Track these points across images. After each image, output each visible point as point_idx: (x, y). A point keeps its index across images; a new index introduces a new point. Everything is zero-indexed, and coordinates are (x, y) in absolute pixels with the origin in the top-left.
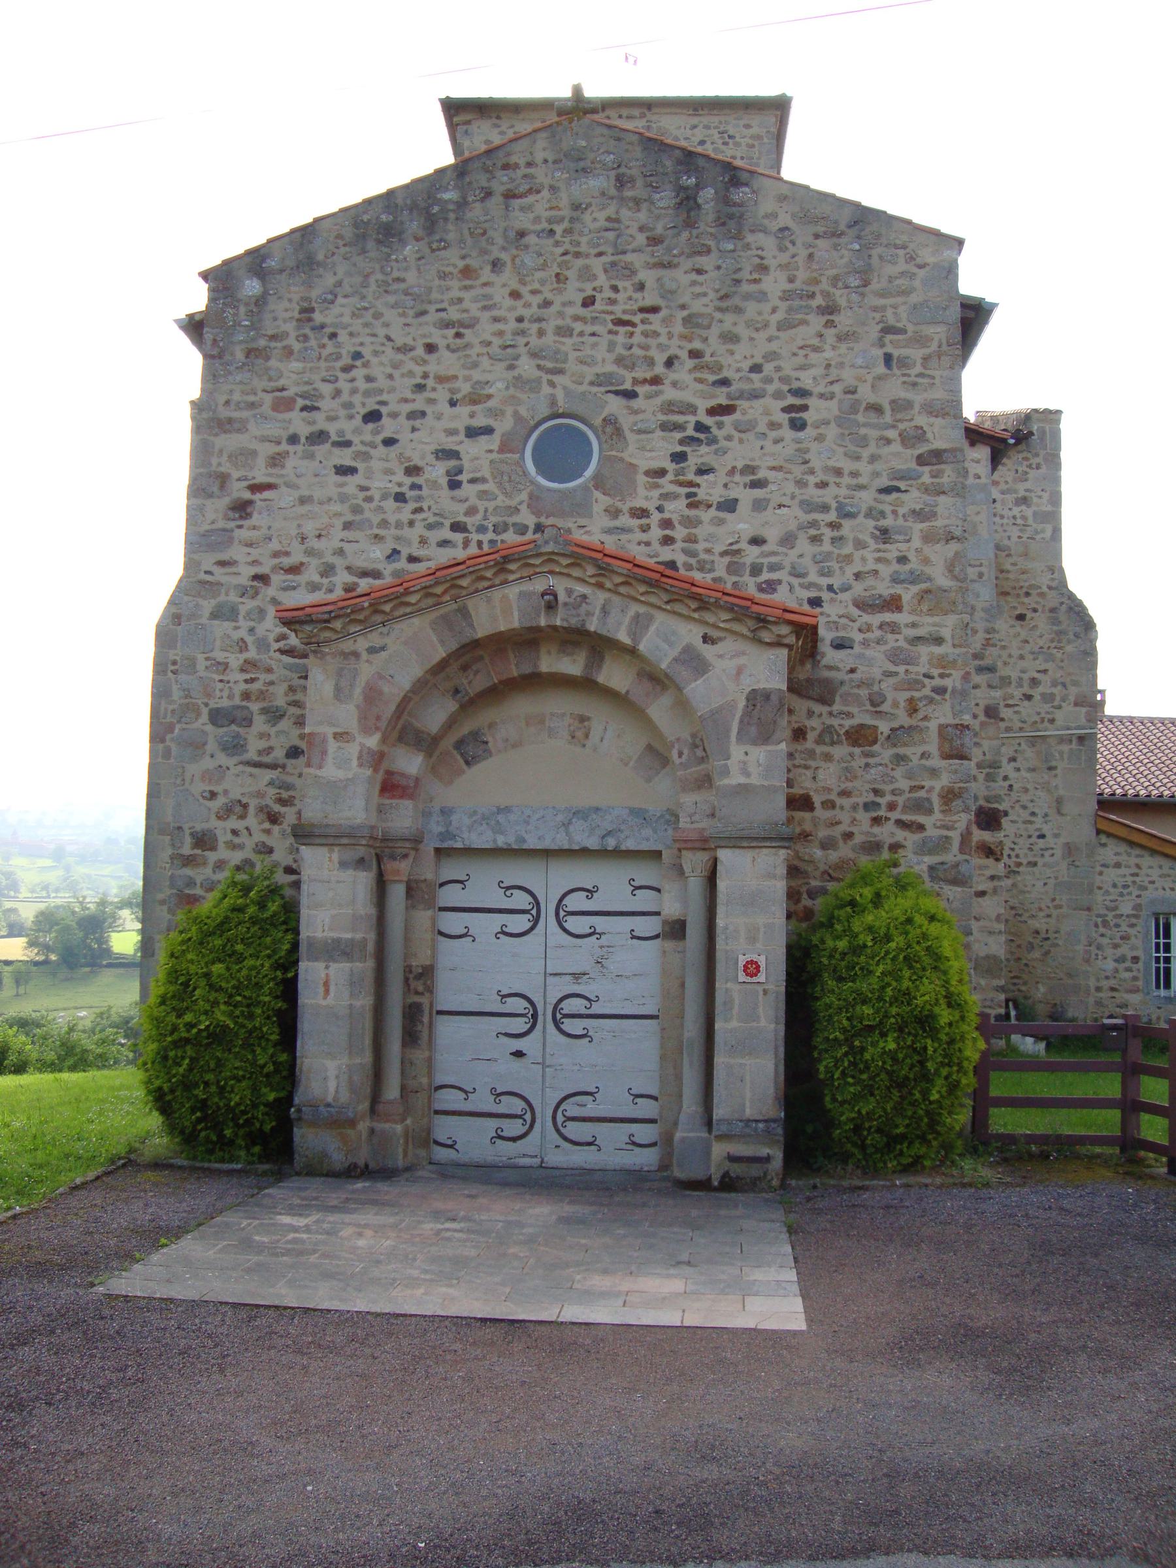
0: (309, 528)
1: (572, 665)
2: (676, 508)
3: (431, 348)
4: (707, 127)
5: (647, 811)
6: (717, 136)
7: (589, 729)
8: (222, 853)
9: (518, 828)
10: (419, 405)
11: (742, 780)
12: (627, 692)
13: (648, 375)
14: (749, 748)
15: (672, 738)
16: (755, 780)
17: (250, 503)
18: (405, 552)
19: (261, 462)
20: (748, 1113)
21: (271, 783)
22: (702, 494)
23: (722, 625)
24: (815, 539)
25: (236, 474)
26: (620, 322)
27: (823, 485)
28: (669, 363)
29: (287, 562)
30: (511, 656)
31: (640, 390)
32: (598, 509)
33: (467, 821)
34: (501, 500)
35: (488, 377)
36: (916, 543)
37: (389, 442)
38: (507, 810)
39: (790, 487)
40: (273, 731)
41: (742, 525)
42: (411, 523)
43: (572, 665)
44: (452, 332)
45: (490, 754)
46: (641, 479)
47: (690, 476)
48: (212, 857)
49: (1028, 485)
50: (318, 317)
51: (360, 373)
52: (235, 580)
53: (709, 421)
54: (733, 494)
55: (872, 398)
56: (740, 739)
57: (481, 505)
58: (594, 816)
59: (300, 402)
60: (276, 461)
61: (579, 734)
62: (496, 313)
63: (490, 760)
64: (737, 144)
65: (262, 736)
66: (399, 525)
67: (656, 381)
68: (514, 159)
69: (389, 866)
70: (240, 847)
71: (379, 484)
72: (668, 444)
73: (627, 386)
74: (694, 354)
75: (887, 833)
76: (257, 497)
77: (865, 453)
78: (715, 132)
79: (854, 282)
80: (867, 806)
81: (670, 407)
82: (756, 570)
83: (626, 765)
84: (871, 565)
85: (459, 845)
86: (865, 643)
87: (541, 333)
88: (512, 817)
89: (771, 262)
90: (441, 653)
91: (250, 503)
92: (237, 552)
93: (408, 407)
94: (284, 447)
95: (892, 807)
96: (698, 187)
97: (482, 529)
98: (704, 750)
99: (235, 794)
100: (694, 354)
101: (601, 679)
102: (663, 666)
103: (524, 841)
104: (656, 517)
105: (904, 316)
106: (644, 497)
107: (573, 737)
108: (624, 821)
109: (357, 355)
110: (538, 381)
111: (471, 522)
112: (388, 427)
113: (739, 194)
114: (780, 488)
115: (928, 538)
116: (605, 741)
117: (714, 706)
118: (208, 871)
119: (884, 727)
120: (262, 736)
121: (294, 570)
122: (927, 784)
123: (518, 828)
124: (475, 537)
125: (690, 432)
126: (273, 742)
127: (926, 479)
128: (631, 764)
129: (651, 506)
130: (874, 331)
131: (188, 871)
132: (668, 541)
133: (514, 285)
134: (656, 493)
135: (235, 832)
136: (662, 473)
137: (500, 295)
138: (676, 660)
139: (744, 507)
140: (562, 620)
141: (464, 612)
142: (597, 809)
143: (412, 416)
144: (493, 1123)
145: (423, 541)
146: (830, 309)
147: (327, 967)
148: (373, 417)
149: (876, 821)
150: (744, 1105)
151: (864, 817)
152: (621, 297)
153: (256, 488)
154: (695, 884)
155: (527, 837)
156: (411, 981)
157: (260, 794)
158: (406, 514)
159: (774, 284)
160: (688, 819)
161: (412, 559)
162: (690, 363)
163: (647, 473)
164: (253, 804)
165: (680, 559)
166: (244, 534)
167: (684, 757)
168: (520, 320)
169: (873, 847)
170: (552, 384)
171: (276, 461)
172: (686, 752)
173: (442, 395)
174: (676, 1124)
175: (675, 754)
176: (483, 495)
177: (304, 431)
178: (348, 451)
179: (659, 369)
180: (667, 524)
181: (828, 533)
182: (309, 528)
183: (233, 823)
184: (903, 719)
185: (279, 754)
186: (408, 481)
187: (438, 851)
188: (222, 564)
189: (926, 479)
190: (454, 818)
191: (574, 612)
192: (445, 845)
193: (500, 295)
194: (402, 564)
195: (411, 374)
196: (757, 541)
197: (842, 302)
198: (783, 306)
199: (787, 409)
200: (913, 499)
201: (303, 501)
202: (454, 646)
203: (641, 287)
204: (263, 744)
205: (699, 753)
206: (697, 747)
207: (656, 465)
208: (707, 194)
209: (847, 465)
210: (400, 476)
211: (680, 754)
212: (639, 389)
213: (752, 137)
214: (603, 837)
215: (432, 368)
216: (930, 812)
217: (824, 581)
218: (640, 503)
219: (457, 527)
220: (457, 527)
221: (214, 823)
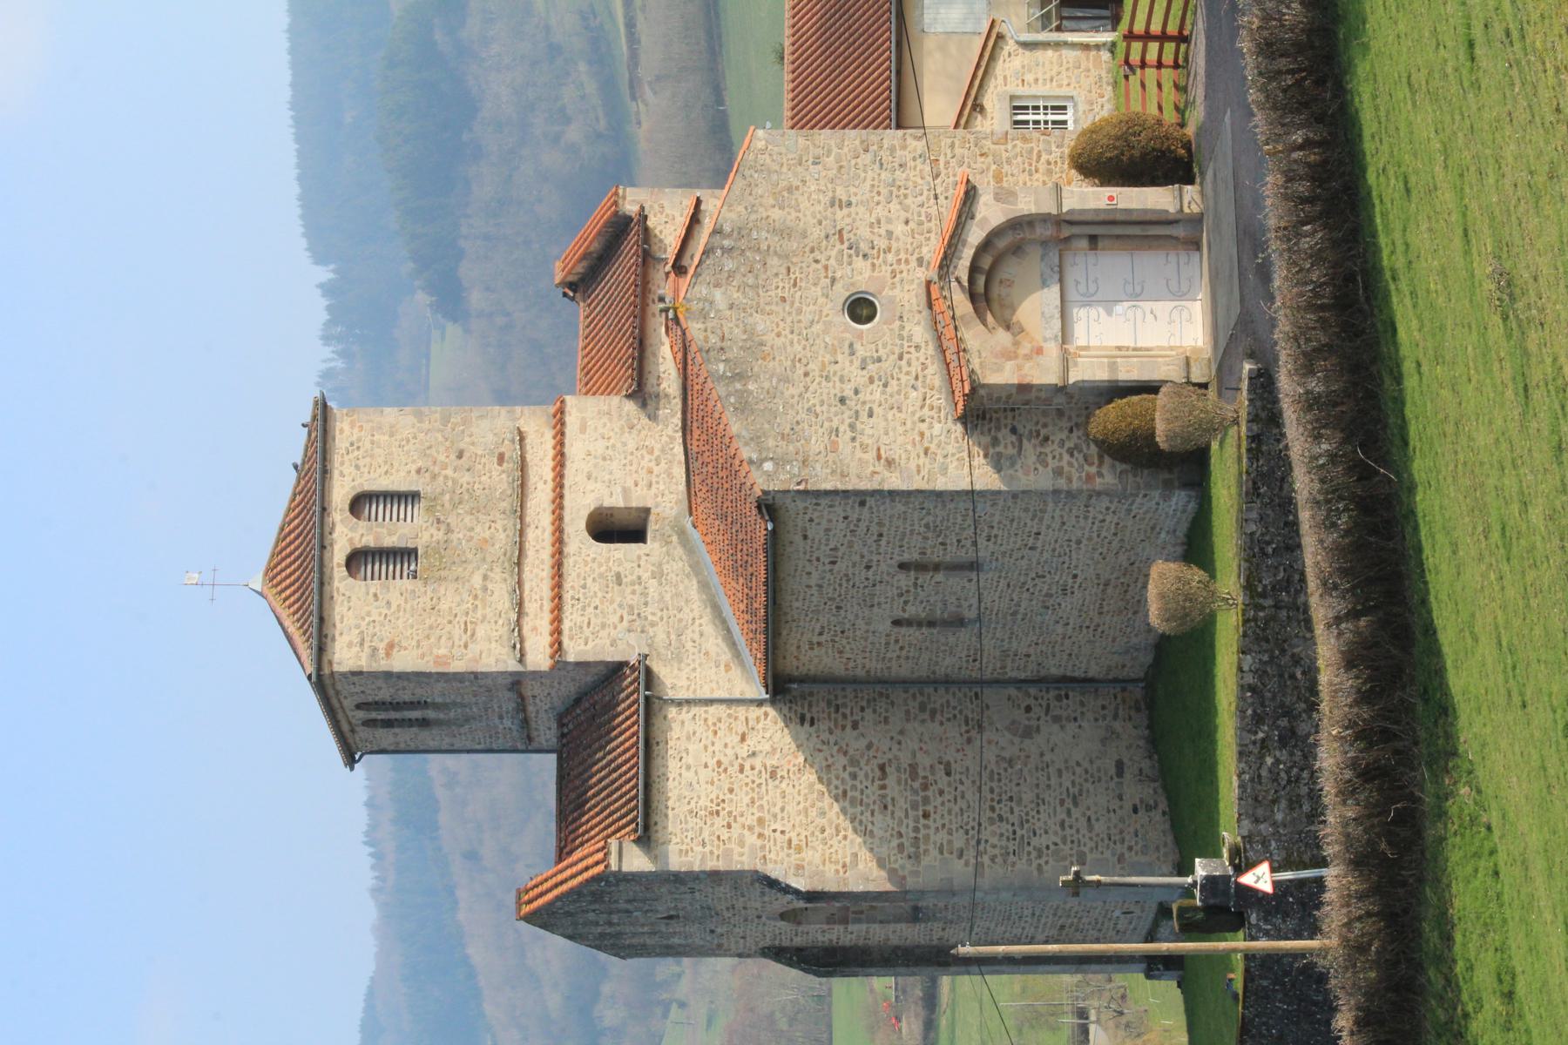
0: (901, 429)
1: (981, 280)
2: (890, 257)
3: (806, 374)
4: (342, 464)
6: (351, 456)
8: (1064, 463)
10: (837, 379)
13: (823, 271)
16: (1032, 199)
17: (887, 460)
18: (913, 382)
19: (865, 456)
20: (1171, 199)
21: (1029, 440)
22: (883, 247)
24: (906, 196)
25: (871, 468)
26: (795, 285)
27: (879, 193)
28: (817, 261)
29: (918, 438)
31: (830, 275)
32: (890, 293)
34: (887, 338)
35: (823, 345)
36: (906, 153)
37: (856, 392)
39: (880, 207)
40: (1003, 442)
41: (899, 229)
42: (898, 379)
43: (981, 280)
44: (798, 365)
46: (876, 274)
47: (875, 251)
48: (1066, 469)
49: (677, 214)
50: (787, 431)
51: (818, 409)
52: (928, 466)
53: (846, 244)
54: (883, 233)
55: (834, 172)
57: (889, 347)
59: (833, 437)
60: (864, 448)
62: (788, 343)
64: (359, 440)
65: (1006, 447)
66: (899, 385)
67: (826, 268)
68: (701, 337)
70: (1061, 454)
71: (877, 396)
72: (859, 263)
73: (828, 281)
74: (812, 251)
75: (1042, 167)
76: (884, 456)
77: (863, 175)
78: (346, 458)
79: (775, 177)
80: (1031, 175)
81: (840, 263)
82: (920, 224)
84: (918, 172)
86: (954, 175)
87: (799, 321)
89: (764, 215)
91: (887, 460)
92: (913, 466)
93: (838, 384)
94: (857, 444)
95: (1031, 165)
96: (722, 248)
97: (902, 345)
99: (1034, 458)
100: (812, 251)
101: (986, 267)
104: (895, 266)
105: (790, 156)
106: (886, 271)
109: (809, 410)
110: (824, 322)
111: (897, 351)
112: (848, 393)
113: (727, 229)
114: (880, 211)
115: (904, 147)
118: (1073, 470)
119: (994, 167)
120: (1006, 447)
121: (922, 434)
122: (1018, 150)
124: (906, 349)
125: (852, 252)
126: (1008, 441)
127: (875, 147)
129: (890, 269)
130: (799, 169)
131: (1075, 479)
132: (907, 261)
133: (773, 335)
134: (884, 268)
135: (1054, 457)
136: (873, 265)
137: (779, 342)
139: (890, 227)
141: (962, 317)
143: (842, 380)
145: (908, 373)
146: (790, 189)
148: (842, 400)
149: (1037, 171)
151: (1036, 176)
152: (781, 285)
153: (879, 457)
154: (1076, 230)
157: (1035, 446)
158: (894, 382)
159: (776, 214)
161: (917, 378)
162: (817, 252)
163: (873, 270)
164: (1039, 449)
165: (916, 256)
166: (903, 462)
168: (792, 332)
169: (1049, 172)
170: (827, 315)
171: (864, 448)
173: (833, 368)
174: (1177, 238)
176: (885, 346)
177: (849, 434)
178: (861, 413)
179: (819, 266)
180: (899, 261)
181: (902, 191)
182: (901, 429)
183: (1049, 459)
184: (991, 158)
185: (1014, 438)
186: (877, 382)
188: (919, 472)
189: (875, 147)
193: (779, 342)
194: (919, 383)
195: (819, 384)
196: (907, 222)
197: (785, 183)
198: (787, 210)
199: (841, 207)
200: (885, 154)
201: (887, 433)
203: (777, 275)
204: (1010, 446)
207: (869, 267)
208: (726, 243)
209: (868, 183)
210: (874, 386)
212: (830, 275)
213: (352, 425)
215: (817, 373)
216: (1032, 148)
217: (926, 193)
218: (888, 275)
219: (901, 358)
220: (901, 358)
221: (1050, 468)
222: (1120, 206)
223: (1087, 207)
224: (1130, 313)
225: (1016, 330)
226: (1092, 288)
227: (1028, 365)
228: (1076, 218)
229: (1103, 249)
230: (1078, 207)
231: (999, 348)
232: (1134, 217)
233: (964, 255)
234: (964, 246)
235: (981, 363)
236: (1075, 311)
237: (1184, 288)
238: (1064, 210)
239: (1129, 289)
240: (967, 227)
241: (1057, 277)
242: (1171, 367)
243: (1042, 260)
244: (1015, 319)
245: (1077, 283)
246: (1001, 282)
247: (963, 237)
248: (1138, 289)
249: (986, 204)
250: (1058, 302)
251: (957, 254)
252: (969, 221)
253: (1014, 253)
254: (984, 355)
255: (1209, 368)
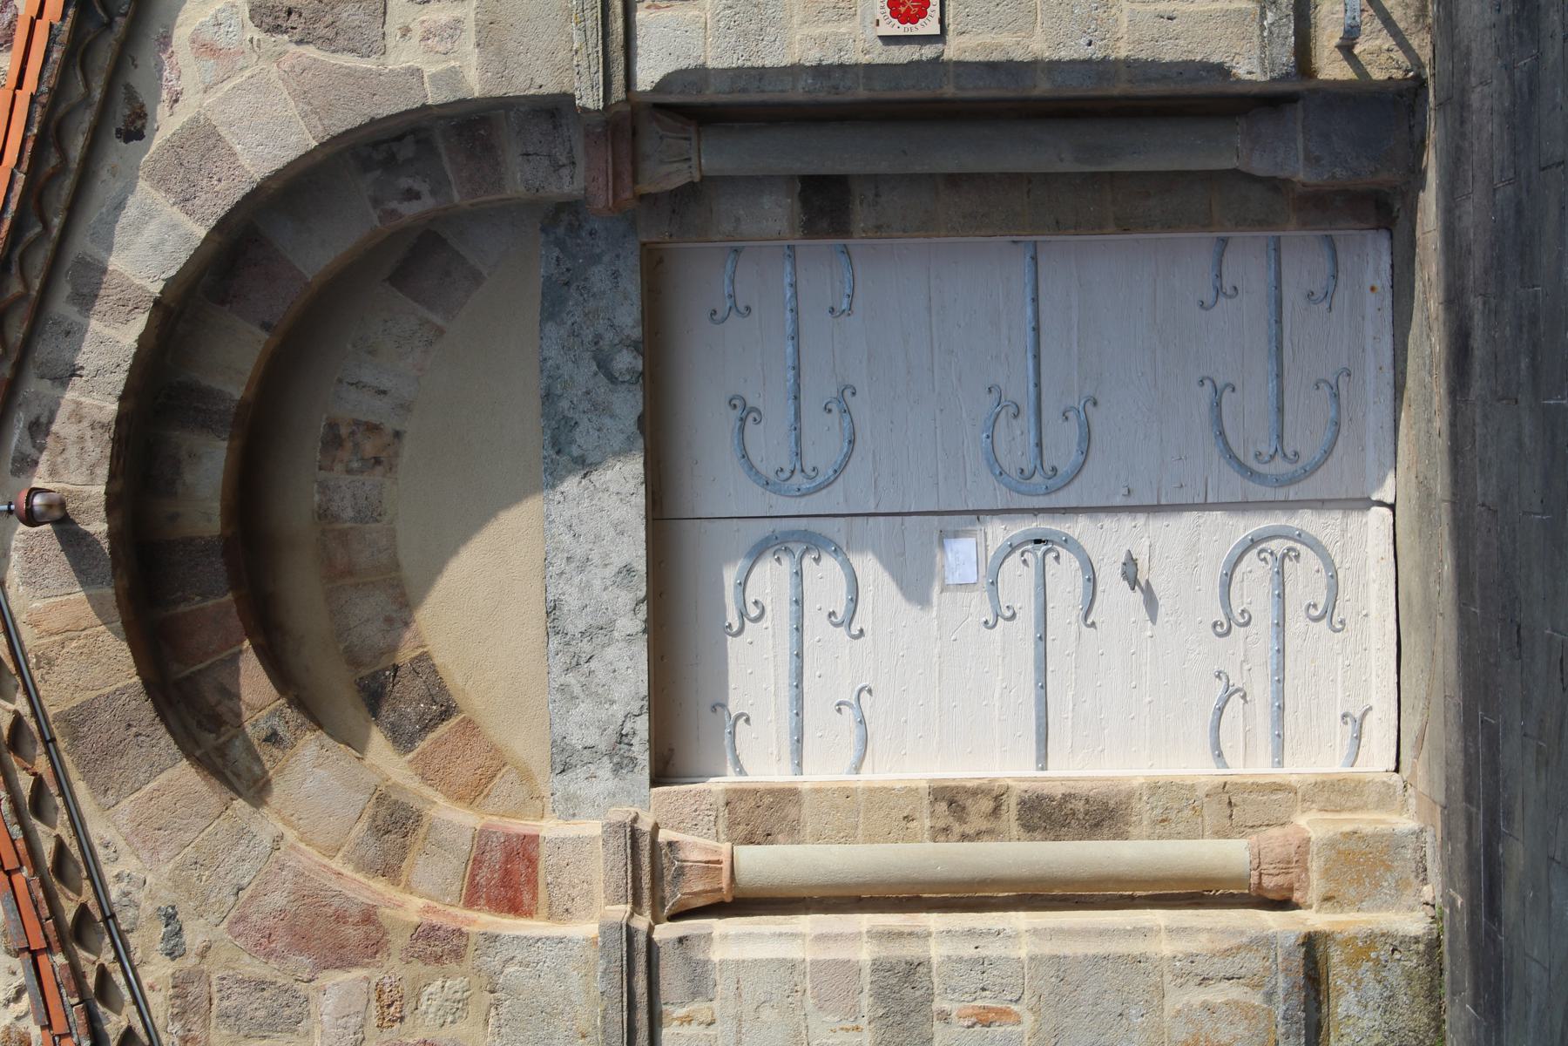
5: (548, 278)
7: (357, 423)
9: (597, 584)
11: (468, 42)
12: (266, 326)
14: (393, 26)
15: (374, 216)
23: (97, 94)
30: (183, 608)
33: (584, 707)
38: (552, 610)
45: (424, 658)
56: (375, 48)
58: (564, 404)
61: (369, 447)
63: (438, 661)
69: (695, 887)
83: (440, 332)
85: (642, 725)
88: (572, 601)
90: (184, 774)
98: (399, 138)
101: (236, 390)
102: (202, 232)
103: (628, 570)
107: (377, 461)
108: (573, 334)
116: (386, 382)
117: (293, 110)
123: (597, 584)
128: (437, 319)
138: (184, 201)
140: (92, 483)
141: (76, 721)
142: (548, 397)
144: (1296, 623)
147: (945, 1017)
150: (1226, 13)
155: (618, 562)
156: (969, 829)
160: (565, 172)
167: (417, 185)
172: (405, 182)
174: (1275, 185)
175: (410, 210)
187: (660, 776)
190: (576, 740)
191: (73, 451)
192: (644, 759)
202: (165, 740)
205: (406, 151)
206: (392, 157)
211: (412, 195)
214: (612, 379)
222: (953, 50)
223: (774, 57)
224: (1017, 578)
225: (407, 700)
226: (823, 449)
227: (439, 989)
228: (712, 94)
229: (879, 230)
230: (719, 55)
231: (278, 899)
232: (1043, 88)
233: (88, 357)
234: (86, 299)
235: (180, 985)
236: (730, 576)
237: (1304, 438)
238: (647, 77)
239: (1015, 445)
240: (104, 187)
241: (628, 405)
242: (1218, 994)
243: (552, 307)
244: (405, 655)
245: (746, 413)
246: (333, 440)
247: (82, 244)
248: (1062, 445)
249: (206, 49)
250: (633, 550)
251: (43, 351)
252: (116, 151)
253: (401, 277)
254: (195, 935)
255: (1432, 994)
